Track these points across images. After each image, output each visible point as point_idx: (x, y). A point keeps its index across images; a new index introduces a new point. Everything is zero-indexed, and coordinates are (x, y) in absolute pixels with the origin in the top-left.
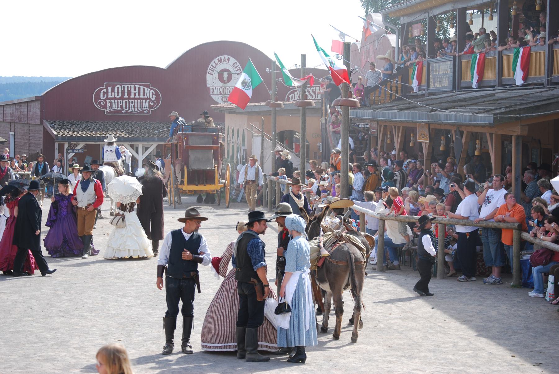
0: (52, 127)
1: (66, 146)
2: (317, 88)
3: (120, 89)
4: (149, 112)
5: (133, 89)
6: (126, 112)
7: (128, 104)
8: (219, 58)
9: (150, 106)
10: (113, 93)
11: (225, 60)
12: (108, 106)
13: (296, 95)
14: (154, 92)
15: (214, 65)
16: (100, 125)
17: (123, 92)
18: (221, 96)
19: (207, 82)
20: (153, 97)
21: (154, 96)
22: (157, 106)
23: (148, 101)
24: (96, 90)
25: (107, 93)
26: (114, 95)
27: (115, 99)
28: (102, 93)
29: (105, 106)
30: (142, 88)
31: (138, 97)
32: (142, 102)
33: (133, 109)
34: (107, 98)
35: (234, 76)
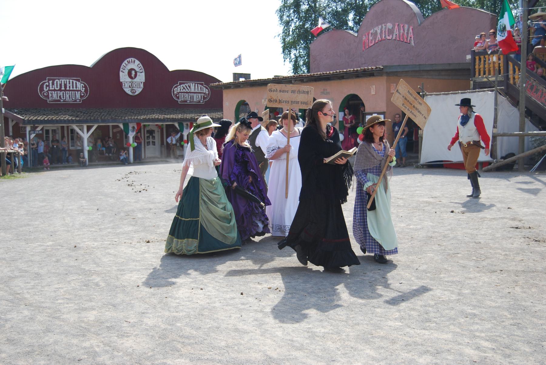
0: (16, 113)
1: (28, 129)
2: (191, 84)
3: (58, 83)
4: (80, 101)
5: (68, 83)
6: (64, 101)
7: (65, 94)
8: (128, 60)
9: (81, 96)
10: (53, 86)
11: (132, 62)
12: (50, 96)
13: (178, 89)
14: (83, 85)
15: (125, 65)
16: (47, 111)
17: (61, 85)
18: (130, 88)
19: (120, 78)
20: (83, 89)
21: (84, 89)
22: (86, 95)
23: (79, 92)
24: (40, 84)
25: (49, 86)
26: (54, 87)
27: (55, 90)
28: (45, 86)
29: (48, 96)
30: (75, 82)
31: (72, 89)
32: (75, 93)
33: (69, 98)
34: (49, 90)
35: (138, 74)
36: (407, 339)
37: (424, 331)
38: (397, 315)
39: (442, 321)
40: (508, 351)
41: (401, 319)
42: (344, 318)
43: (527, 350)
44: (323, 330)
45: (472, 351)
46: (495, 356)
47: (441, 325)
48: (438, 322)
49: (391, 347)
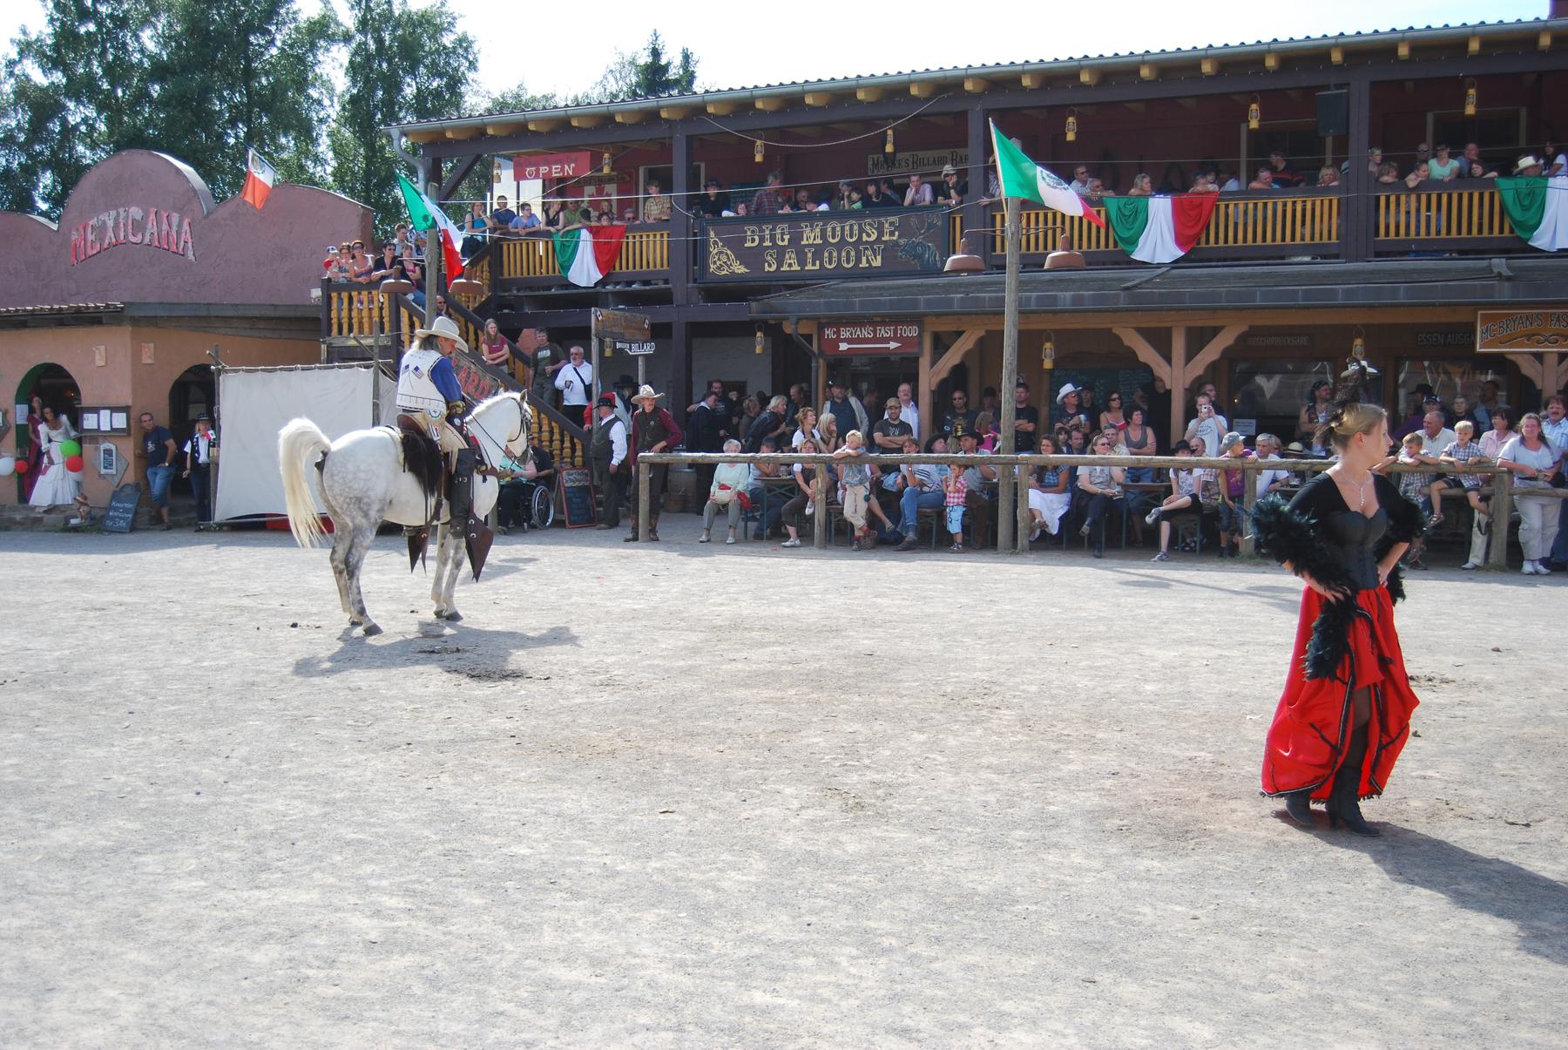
36: (219, 914)
37: (257, 893)
38: (193, 864)
39: (296, 865)
40: (438, 911)
41: (203, 871)
42: (65, 886)
43: (478, 901)
44: (16, 923)
45: (366, 921)
46: (414, 923)
47: (295, 874)
48: (286, 868)
49: (186, 938)
